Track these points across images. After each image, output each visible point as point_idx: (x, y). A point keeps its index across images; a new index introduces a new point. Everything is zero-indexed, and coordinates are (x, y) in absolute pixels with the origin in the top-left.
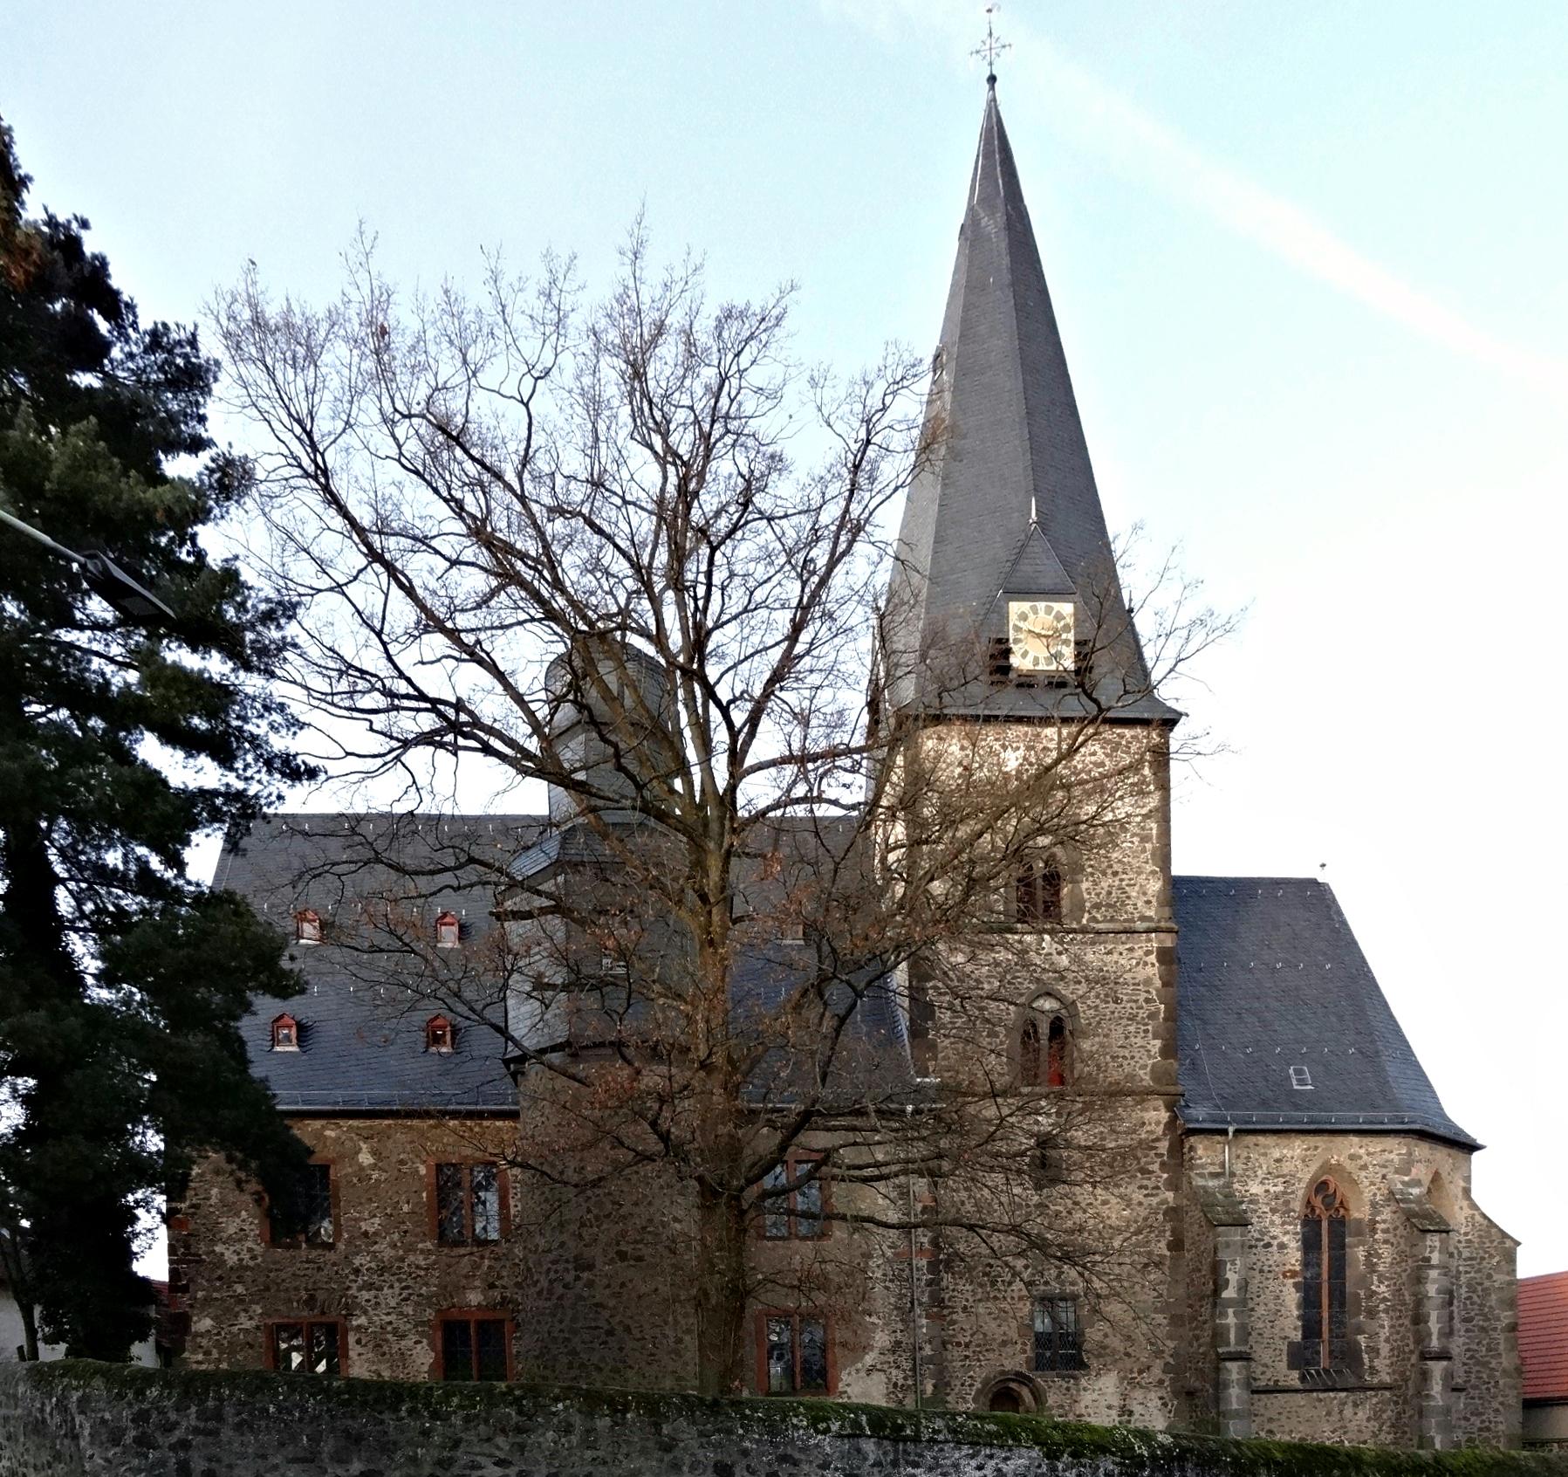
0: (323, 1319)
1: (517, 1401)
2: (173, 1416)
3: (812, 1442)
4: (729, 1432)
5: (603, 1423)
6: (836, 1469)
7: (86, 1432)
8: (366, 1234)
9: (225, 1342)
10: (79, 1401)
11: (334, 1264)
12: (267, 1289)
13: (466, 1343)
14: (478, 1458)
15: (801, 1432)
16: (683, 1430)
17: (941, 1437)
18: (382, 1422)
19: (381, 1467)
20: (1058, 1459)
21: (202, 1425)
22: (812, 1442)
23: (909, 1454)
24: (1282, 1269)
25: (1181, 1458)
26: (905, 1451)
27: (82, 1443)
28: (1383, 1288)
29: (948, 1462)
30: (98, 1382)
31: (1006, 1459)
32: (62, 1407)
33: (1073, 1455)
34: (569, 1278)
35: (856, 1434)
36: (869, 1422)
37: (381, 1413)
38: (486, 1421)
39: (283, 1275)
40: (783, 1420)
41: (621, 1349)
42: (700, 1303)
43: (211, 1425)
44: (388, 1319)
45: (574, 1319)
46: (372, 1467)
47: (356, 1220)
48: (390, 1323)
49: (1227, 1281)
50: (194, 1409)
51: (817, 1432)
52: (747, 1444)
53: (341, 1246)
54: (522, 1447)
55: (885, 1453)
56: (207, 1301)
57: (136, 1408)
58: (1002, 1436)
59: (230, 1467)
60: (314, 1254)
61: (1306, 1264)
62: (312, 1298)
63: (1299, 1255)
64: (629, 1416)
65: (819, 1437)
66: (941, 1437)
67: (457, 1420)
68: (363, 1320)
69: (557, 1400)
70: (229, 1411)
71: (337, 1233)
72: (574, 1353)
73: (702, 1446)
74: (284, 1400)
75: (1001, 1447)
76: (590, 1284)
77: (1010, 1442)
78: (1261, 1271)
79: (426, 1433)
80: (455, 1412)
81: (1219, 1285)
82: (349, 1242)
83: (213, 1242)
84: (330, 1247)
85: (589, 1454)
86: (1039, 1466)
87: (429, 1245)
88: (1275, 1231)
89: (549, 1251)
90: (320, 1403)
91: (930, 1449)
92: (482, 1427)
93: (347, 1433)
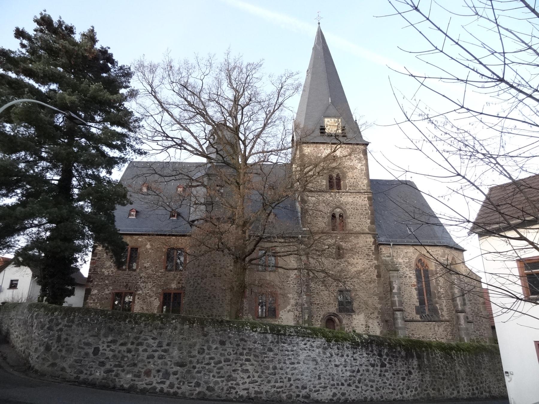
0: (130, 291)
1: (162, 319)
2: (60, 321)
3: (251, 334)
4: (225, 331)
5: (186, 327)
6: (259, 343)
7: (35, 325)
8: (145, 267)
9: (100, 297)
10: (36, 315)
11: (135, 276)
12: (115, 282)
13: (170, 299)
14: (148, 337)
15: (248, 331)
16: (210, 329)
17: (292, 334)
19: (117, 339)
20: (330, 342)
21: (67, 324)
22: (251, 334)
23: (282, 339)
24: (411, 284)
25: (371, 343)
27: (34, 328)
28: (442, 290)
29: (295, 342)
30: (42, 310)
31: (314, 342)
32: (32, 317)
33: (336, 341)
34: (199, 281)
35: (266, 332)
36: (270, 329)
37: (120, 322)
38: (151, 325)
39: (120, 278)
40: (242, 327)
41: (212, 303)
42: (232, 289)
43: (70, 324)
44: (148, 292)
45: (199, 294)
46: (114, 339)
47: (144, 263)
48: (148, 293)
49: (394, 287)
50: (66, 319)
51: (253, 331)
52: (230, 335)
53: (138, 270)
54: (161, 334)
55: (275, 339)
56: (97, 285)
57: (50, 318)
58: (312, 334)
59: (73, 337)
60: (130, 272)
61: (418, 283)
62: (127, 285)
63: (415, 280)
64: (194, 325)
65: (254, 333)
66: (292, 334)
67: (142, 325)
68: (140, 292)
69: (173, 319)
70: (76, 319)
71: (137, 267)
72: (198, 303)
73: (216, 335)
74: (93, 317)
75: (312, 338)
76: (205, 284)
77: (315, 336)
78: (405, 284)
79: (133, 328)
80: (142, 322)
81: (392, 288)
82: (140, 269)
83: (102, 268)
84: (135, 270)
85: (181, 336)
86: (324, 344)
87: (162, 271)
88: (408, 273)
89: (195, 273)
90: (103, 318)
91: (289, 338)
92: (150, 327)
93: (109, 328)
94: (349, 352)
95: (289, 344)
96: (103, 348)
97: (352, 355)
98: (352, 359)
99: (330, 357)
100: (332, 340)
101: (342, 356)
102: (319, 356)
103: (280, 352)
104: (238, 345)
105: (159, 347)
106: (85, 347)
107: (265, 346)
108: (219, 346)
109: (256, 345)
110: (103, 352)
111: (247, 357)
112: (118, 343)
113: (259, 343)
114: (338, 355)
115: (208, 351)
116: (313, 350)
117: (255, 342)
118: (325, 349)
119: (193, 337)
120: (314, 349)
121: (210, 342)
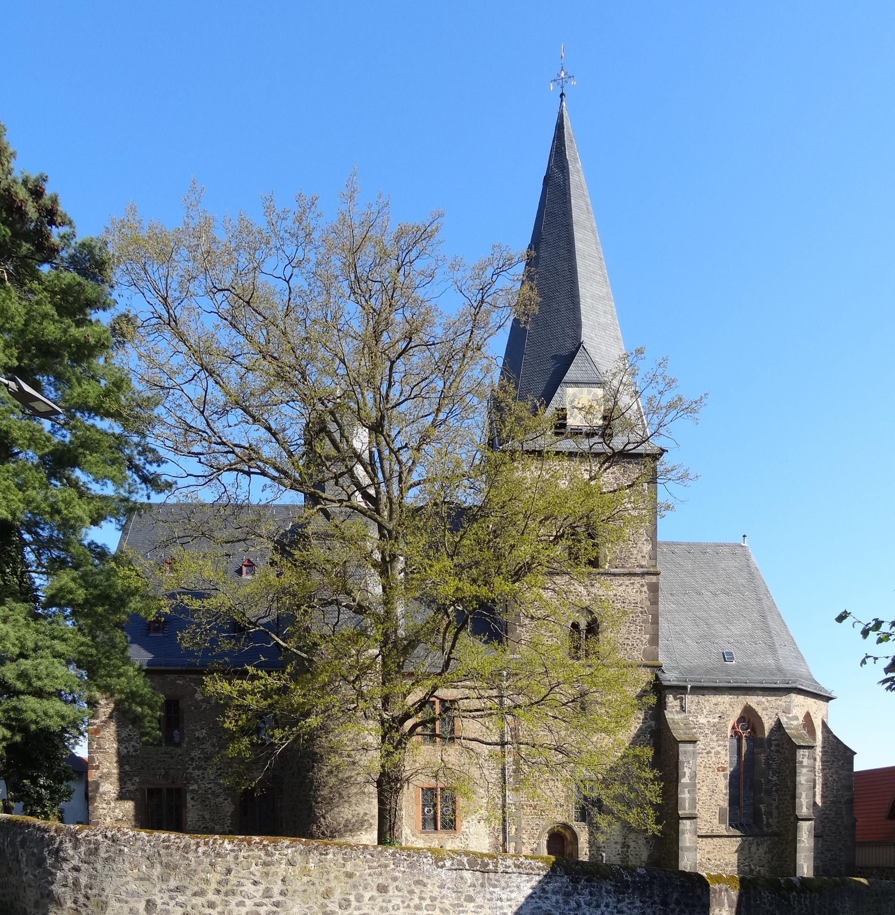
3: (435, 872)
4: (386, 866)
6: (449, 888)
17: (510, 870)
18: (187, 859)
20: (578, 883)
26: (488, 878)
51: (438, 867)
55: (477, 880)
79: (212, 865)
86: (567, 887)
94: (610, 900)
95: (503, 889)
96: (162, 901)
97: (615, 905)
98: (615, 911)
99: (575, 909)
100: (582, 878)
101: (598, 906)
102: (558, 908)
103: (486, 901)
104: (411, 892)
105: (264, 898)
106: (128, 899)
107: (460, 892)
108: (377, 895)
109: (444, 891)
110: (164, 907)
111: (428, 913)
112: (189, 893)
113: (449, 888)
114: (589, 905)
115: (358, 904)
116: (547, 898)
117: (442, 886)
118: (568, 895)
119: (328, 880)
120: (549, 895)
121: (361, 888)
